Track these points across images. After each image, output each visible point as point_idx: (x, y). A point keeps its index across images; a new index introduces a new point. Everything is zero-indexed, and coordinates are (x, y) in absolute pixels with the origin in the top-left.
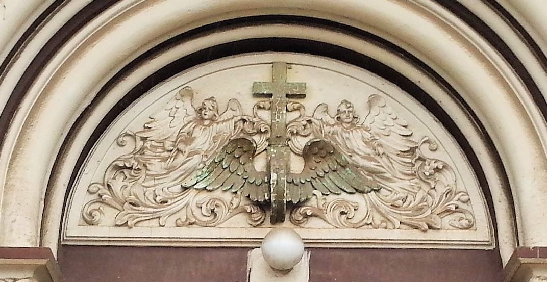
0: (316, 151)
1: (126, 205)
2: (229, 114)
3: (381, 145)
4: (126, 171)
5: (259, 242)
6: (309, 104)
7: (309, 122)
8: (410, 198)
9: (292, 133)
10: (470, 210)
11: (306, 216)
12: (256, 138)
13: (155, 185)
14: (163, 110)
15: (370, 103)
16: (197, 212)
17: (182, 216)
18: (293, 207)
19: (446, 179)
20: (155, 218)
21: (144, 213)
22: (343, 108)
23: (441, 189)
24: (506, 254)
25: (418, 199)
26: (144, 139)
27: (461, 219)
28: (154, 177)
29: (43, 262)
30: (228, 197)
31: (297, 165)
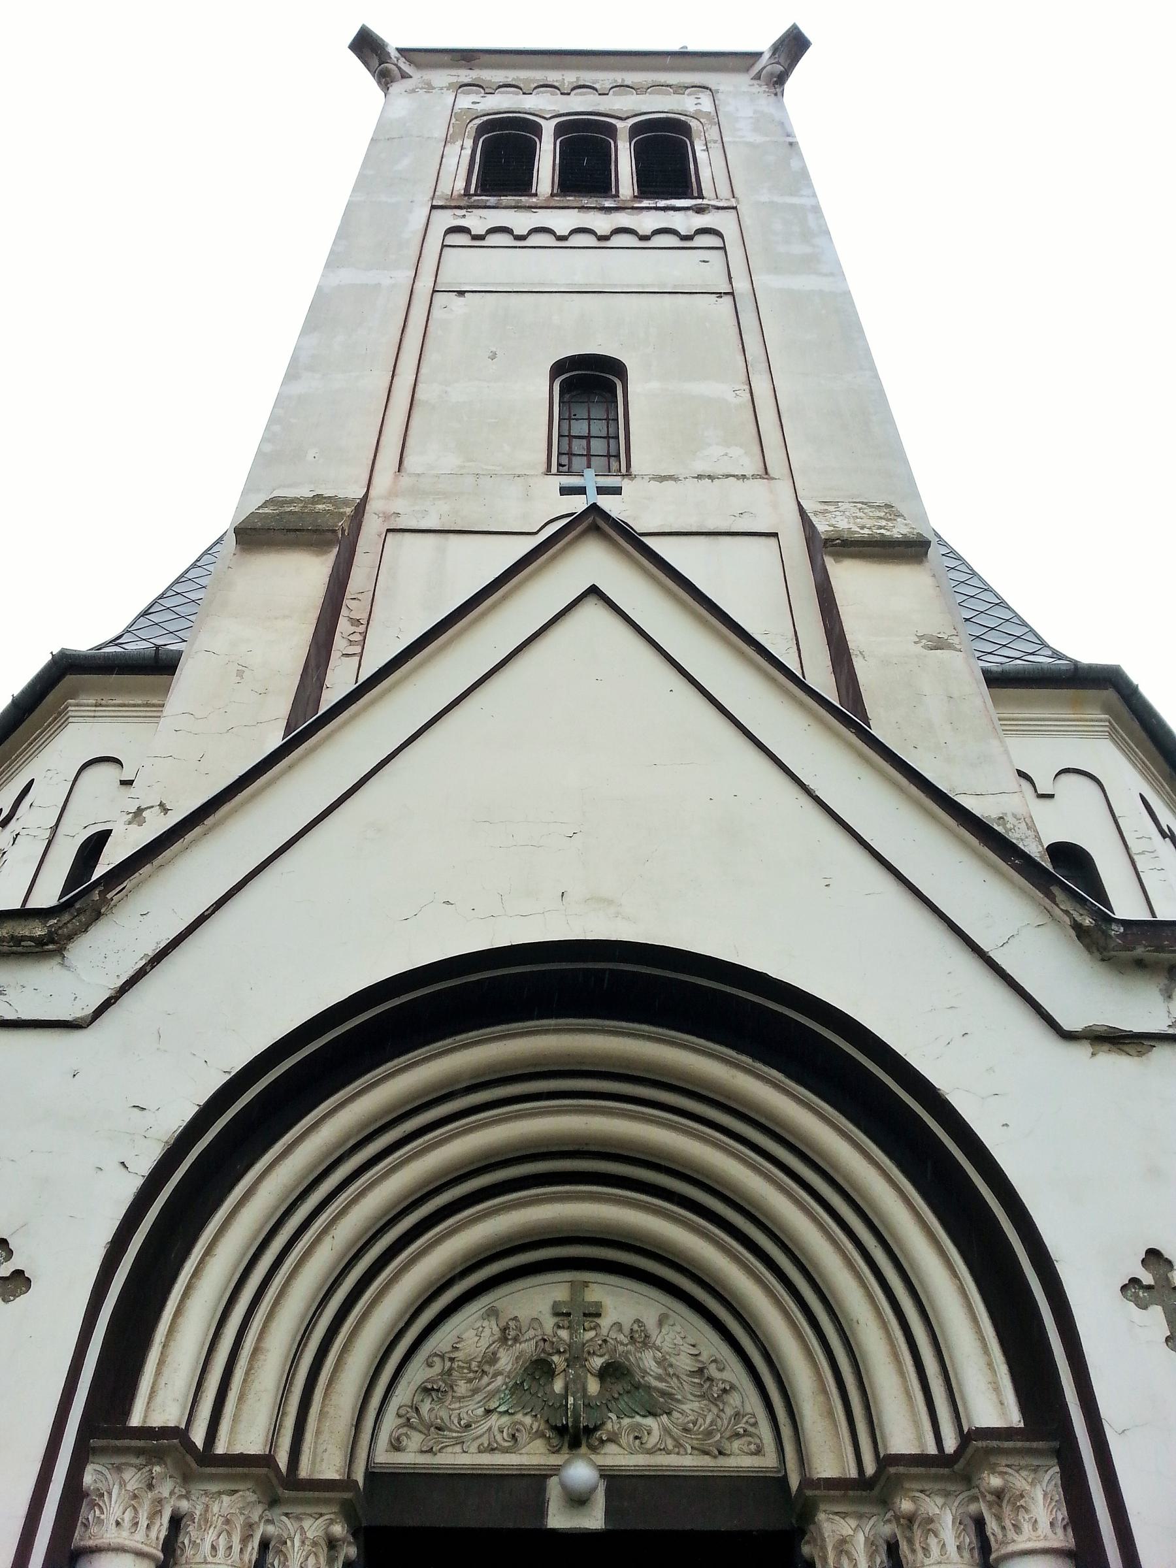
0: (613, 1372)
2: (531, 1333)
3: (671, 1365)
4: (434, 1394)
5: (556, 1470)
6: (605, 1322)
7: (605, 1341)
8: (700, 1421)
9: (589, 1353)
10: (756, 1432)
11: (602, 1442)
12: (555, 1358)
13: (460, 1408)
14: (469, 1332)
15: (660, 1323)
16: (499, 1437)
17: (485, 1441)
18: (589, 1431)
22: (636, 1327)
23: (729, 1412)
25: (708, 1421)
26: (452, 1360)
27: (750, 1443)
28: (461, 1399)
29: (347, 1495)
30: (528, 1420)
31: (593, 1386)
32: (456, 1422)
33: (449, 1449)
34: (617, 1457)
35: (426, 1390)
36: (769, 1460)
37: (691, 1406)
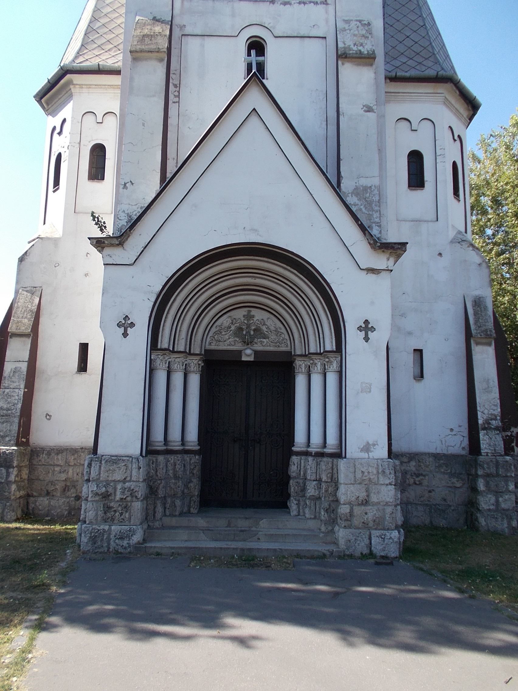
6: (255, 319)
14: (225, 321)
18: (251, 343)
19: (283, 336)
24: (293, 353)
30: (238, 339)
31: (252, 333)
34: (258, 347)
36: (288, 349)
37: (273, 337)
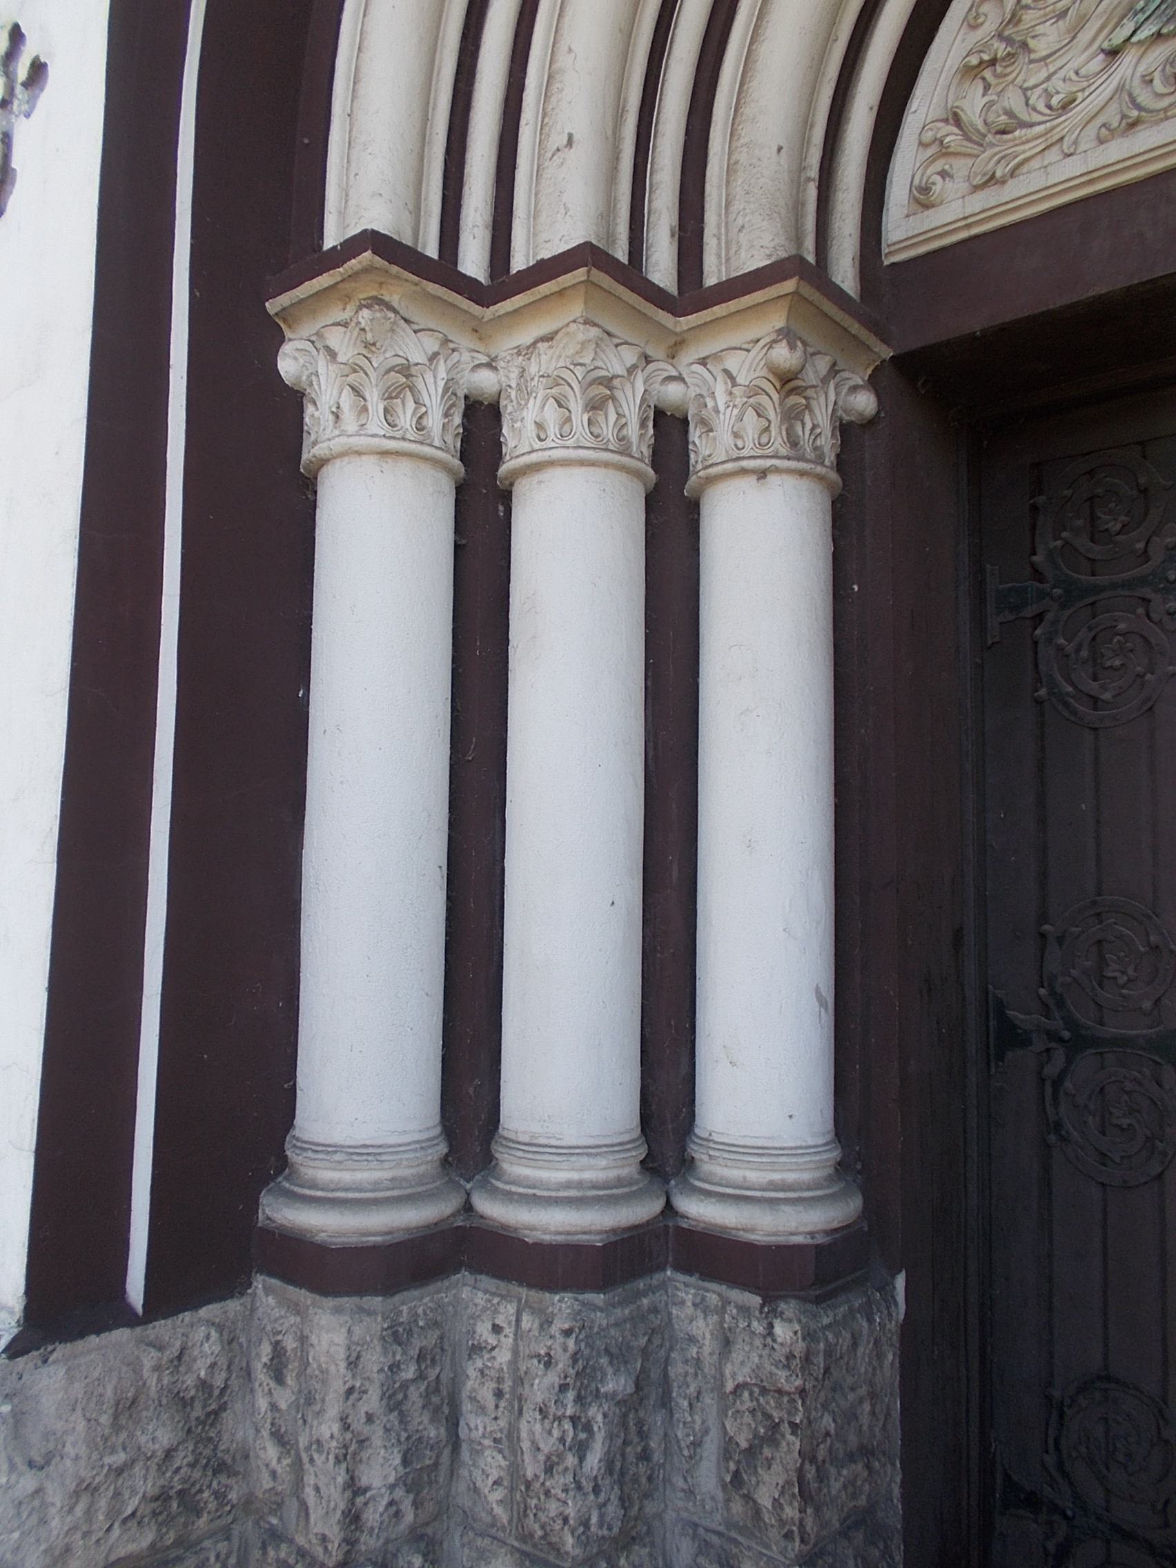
1: (990, 138)
4: (987, 74)
13: (1048, 78)
16: (1144, 98)
17: (1112, 116)
20: (1051, 145)
21: (1028, 141)
32: (1041, 107)
33: (1035, 164)
35: (970, 72)
